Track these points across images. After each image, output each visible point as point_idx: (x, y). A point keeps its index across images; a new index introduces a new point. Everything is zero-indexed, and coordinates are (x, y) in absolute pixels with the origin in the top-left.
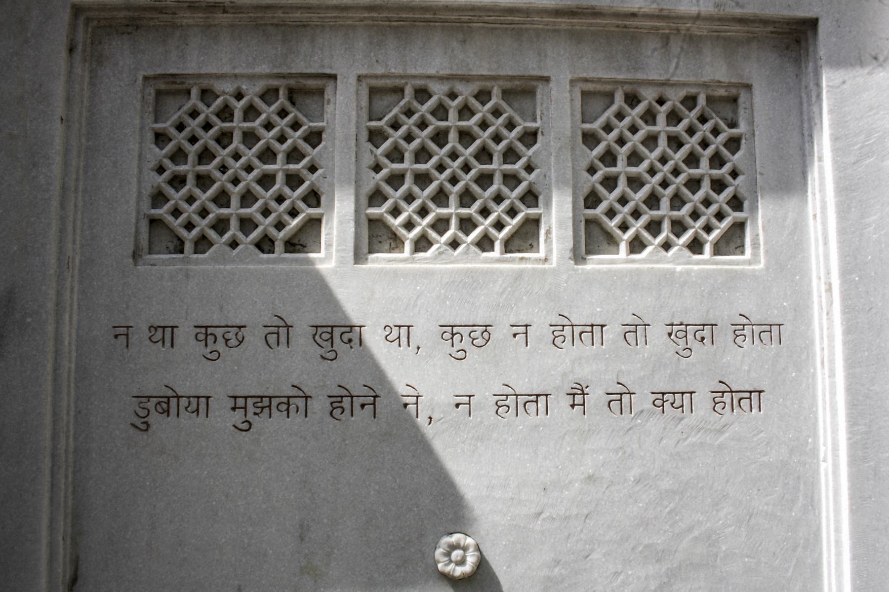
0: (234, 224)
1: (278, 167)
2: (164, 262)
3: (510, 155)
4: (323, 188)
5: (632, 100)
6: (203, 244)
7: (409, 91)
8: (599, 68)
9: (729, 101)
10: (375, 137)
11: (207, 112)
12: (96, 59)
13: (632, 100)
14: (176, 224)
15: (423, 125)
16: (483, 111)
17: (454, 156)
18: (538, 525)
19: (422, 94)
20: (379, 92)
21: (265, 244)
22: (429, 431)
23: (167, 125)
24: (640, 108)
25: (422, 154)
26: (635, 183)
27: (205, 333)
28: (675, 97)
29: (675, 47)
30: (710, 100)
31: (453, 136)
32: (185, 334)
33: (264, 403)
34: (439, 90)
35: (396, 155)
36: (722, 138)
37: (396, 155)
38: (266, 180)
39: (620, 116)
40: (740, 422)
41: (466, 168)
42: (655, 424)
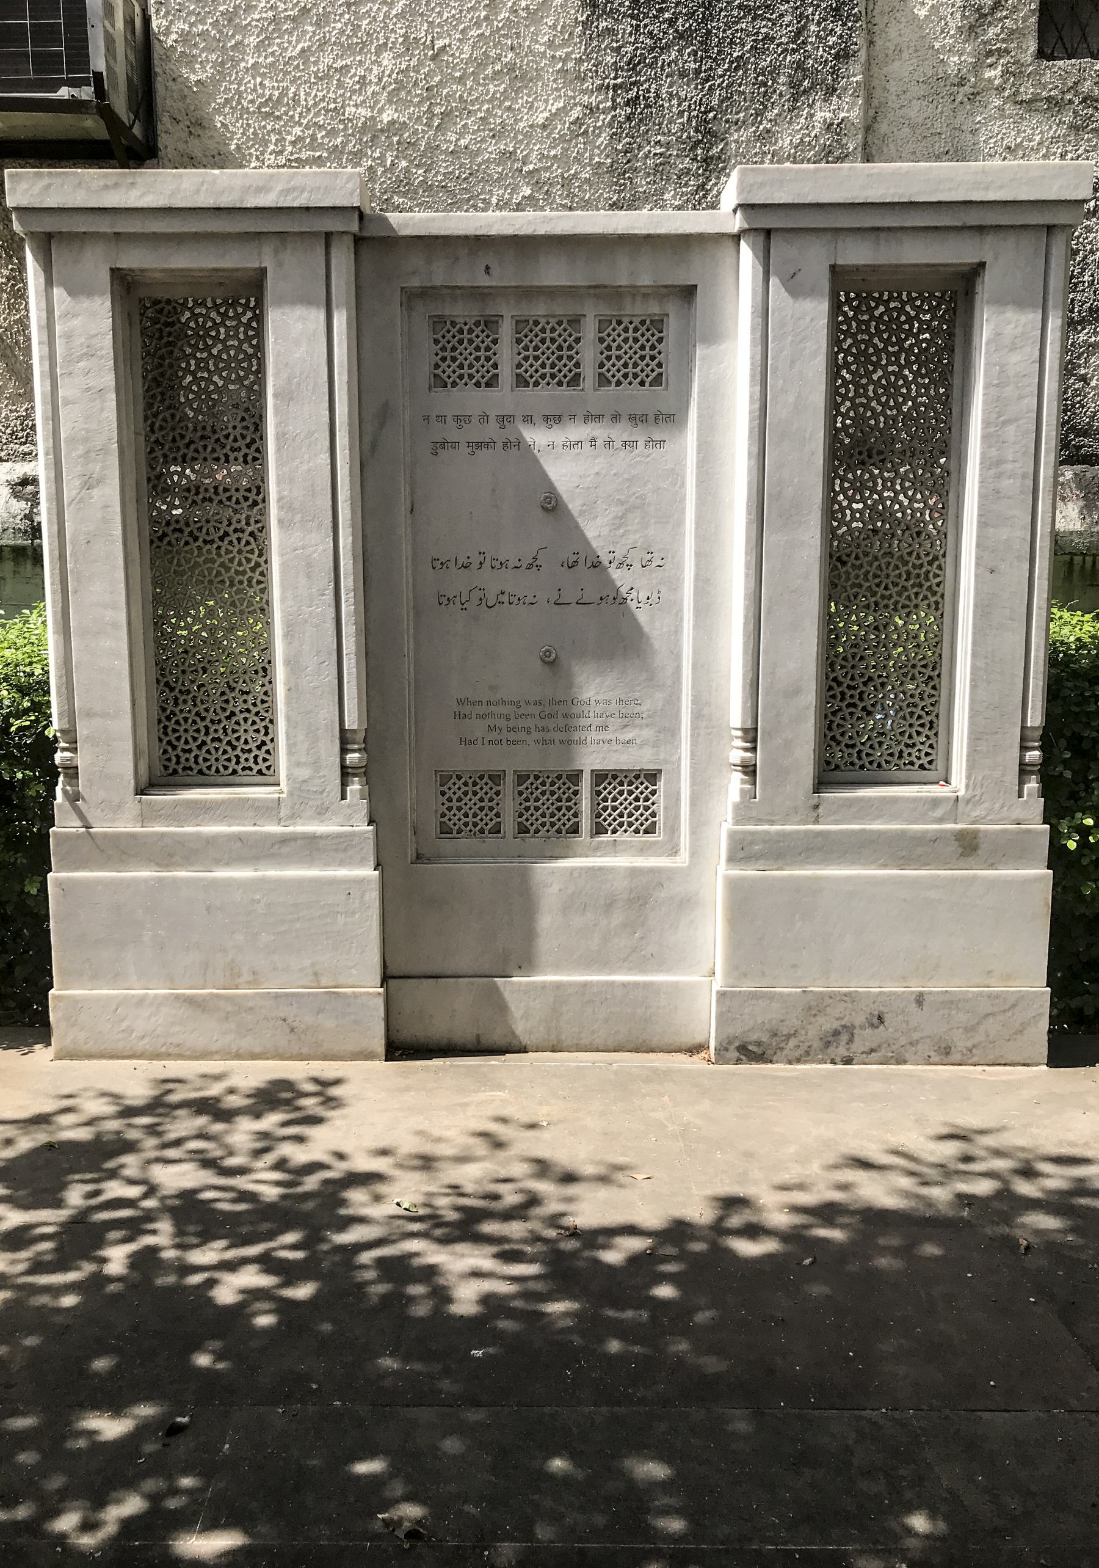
0: (466, 376)
1: (482, 353)
2: (440, 393)
3: (570, 348)
4: (499, 363)
5: (619, 323)
6: (454, 384)
7: (531, 322)
8: (607, 311)
9: (658, 324)
10: (519, 341)
11: (454, 331)
12: (410, 309)
13: (619, 323)
14: (444, 376)
15: (536, 336)
16: (560, 330)
17: (548, 348)
18: (577, 490)
19: (536, 323)
20: (520, 323)
21: (478, 384)
22: (538, 455)
23: (438, 336)
24: (622, 326)
25: (536, 348)
26: (619, 358)
27: (457, 418)
28: (636, 321)
29: (639, 299)
30: (651, 321)
31: (548, 340)
32: (449, 419)
33: (479, 445)
34: (543, 321)
35: (526, 348)
36: (655, 338)
37: (526, 348)
38: (477, 359)
39: (614, 330)
40: (656, 453)
41: (553, 353)
42: (622, 454)
